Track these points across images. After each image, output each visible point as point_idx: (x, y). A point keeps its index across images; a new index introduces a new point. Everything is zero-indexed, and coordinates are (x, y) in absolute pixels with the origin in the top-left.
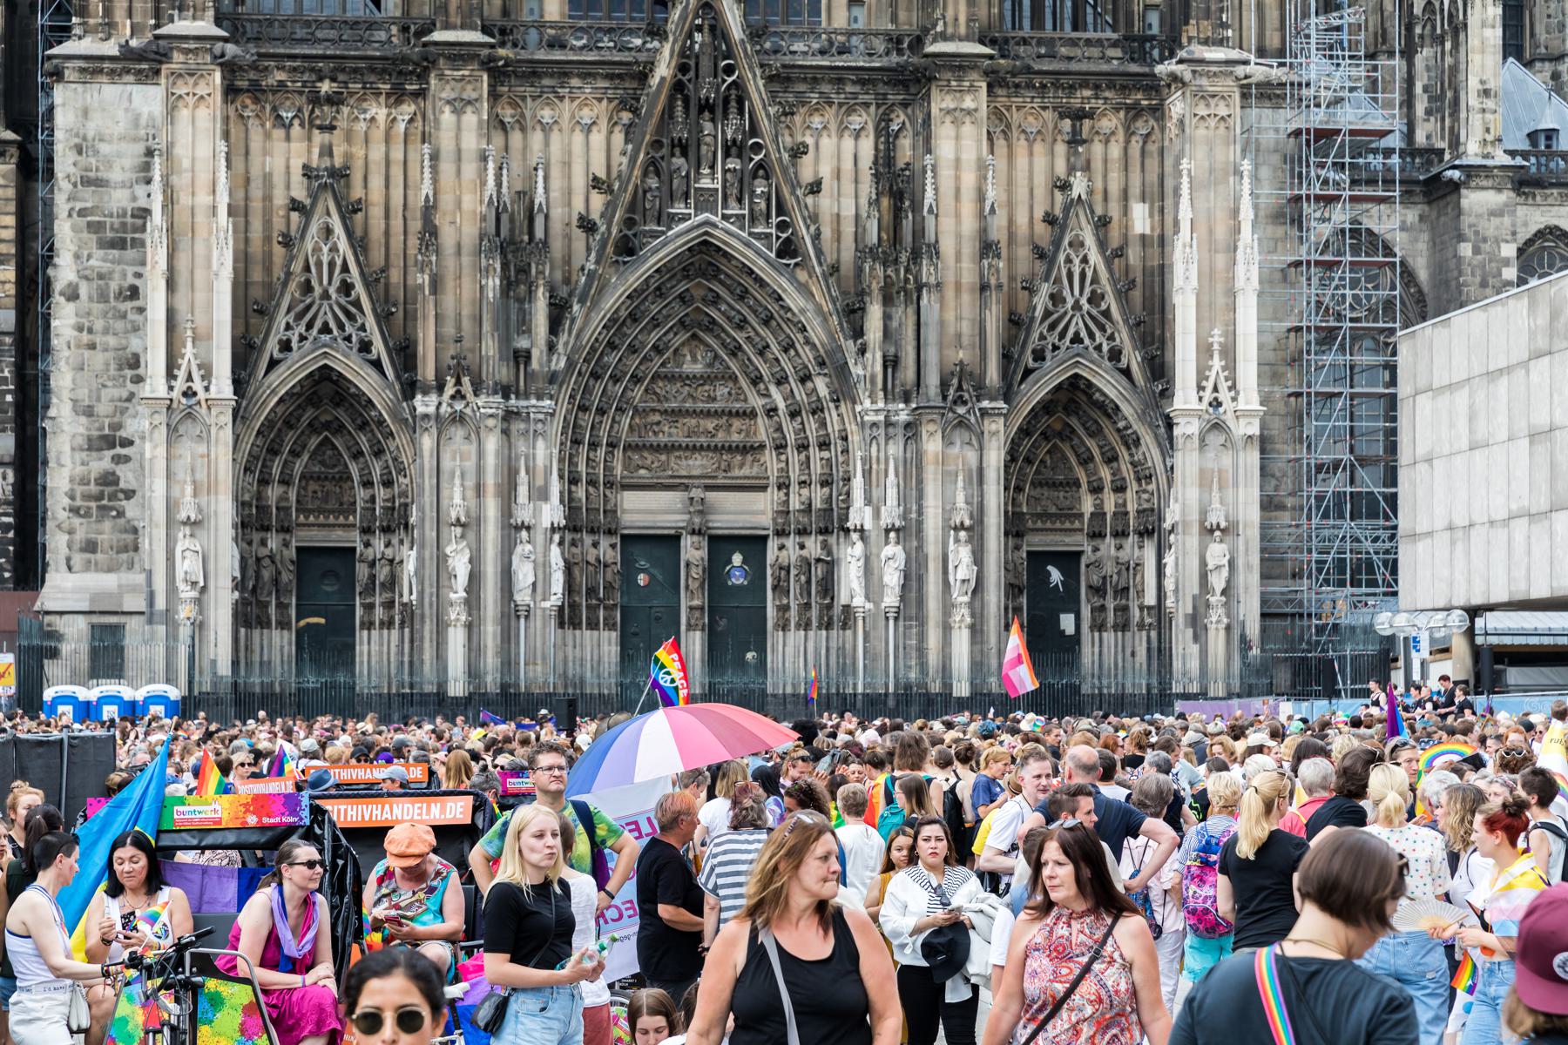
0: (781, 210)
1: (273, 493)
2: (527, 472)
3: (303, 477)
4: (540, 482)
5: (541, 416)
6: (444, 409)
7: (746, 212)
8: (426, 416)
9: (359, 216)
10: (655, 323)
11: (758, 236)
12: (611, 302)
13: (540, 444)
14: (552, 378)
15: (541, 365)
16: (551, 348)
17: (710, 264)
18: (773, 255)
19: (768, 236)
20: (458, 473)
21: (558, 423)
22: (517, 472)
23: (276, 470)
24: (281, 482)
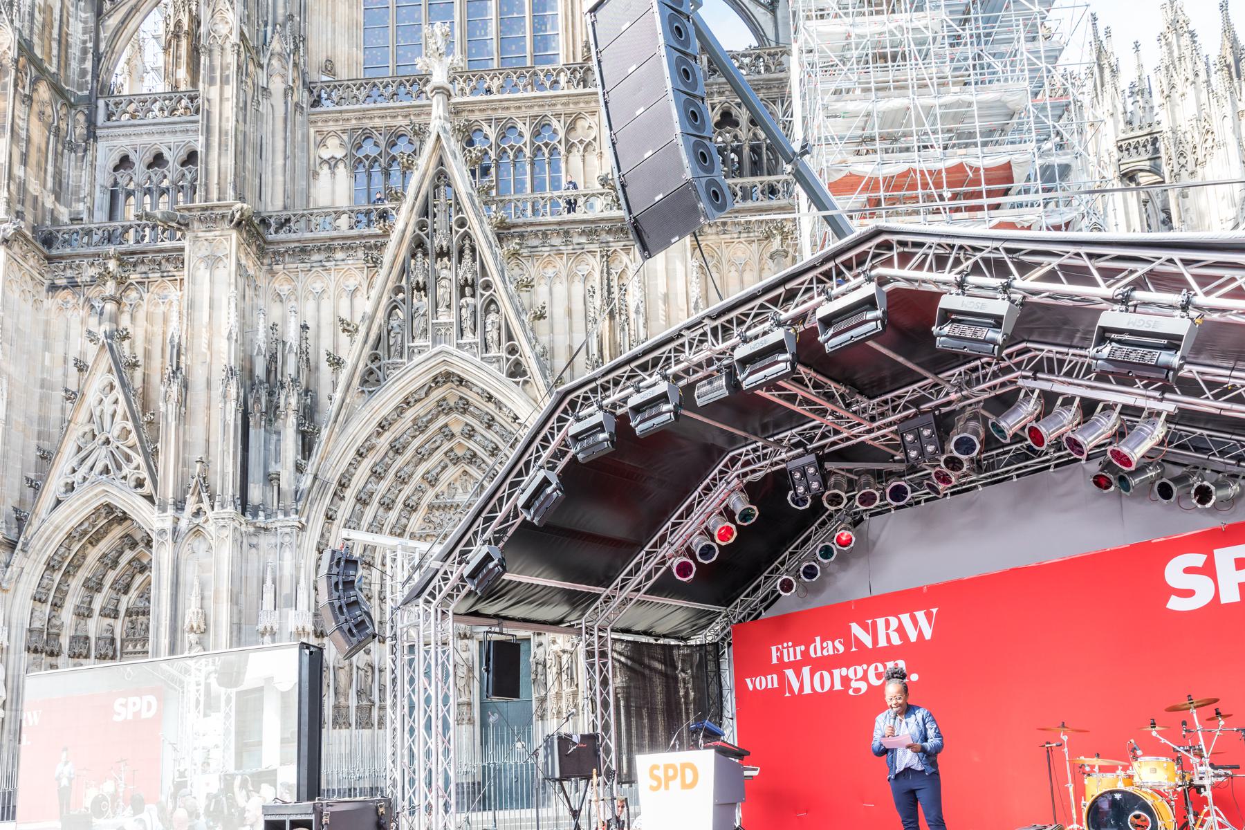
0: (510, 337)
1: (94, 627)
2: (274, 582)
3: (129, 613)
4: (286, 589)
5: (288, 530)
6: (184, 525)
7: (478, 340)
8: (162, 532)
9: (138, 373)
10: (421, 457)
11: (490, 361)
12: (360, 429)
13: (288, 555)
14: (298, 495)
15: (290, 485)
16: (299, 469)
17: (461, 398)
18: (504, 375)
19: (498, 360)
20: (196, 583)
21: (312, 537)
22: (263, 582)
23: (97, 606)
24: (103, 614)
